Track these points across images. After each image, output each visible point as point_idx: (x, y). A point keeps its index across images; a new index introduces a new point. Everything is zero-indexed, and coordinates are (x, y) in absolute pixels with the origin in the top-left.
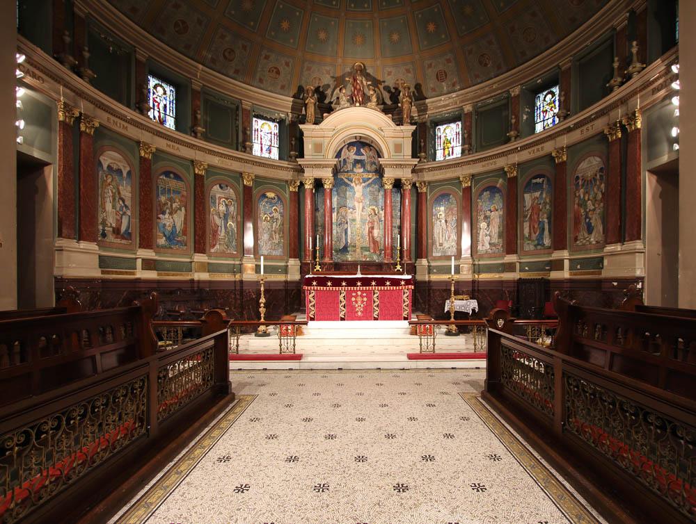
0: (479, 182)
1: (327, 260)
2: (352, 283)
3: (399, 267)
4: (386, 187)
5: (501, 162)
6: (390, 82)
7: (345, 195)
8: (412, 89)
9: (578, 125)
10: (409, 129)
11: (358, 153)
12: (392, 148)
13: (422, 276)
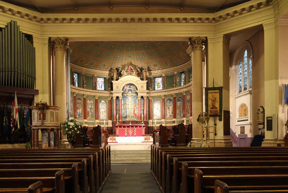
0: (167, 97)
1: (121, 120)
2: (128, 127)
3: (143, 122)
4: (139, 99)
5: (172, 93)
6: (140, 66)
7: (126, 100)
8: (147, 68)
9: (186, 87)
10: (145, 82)
11: (130, 87)
12: (140, 87)
13: (150, 125)
